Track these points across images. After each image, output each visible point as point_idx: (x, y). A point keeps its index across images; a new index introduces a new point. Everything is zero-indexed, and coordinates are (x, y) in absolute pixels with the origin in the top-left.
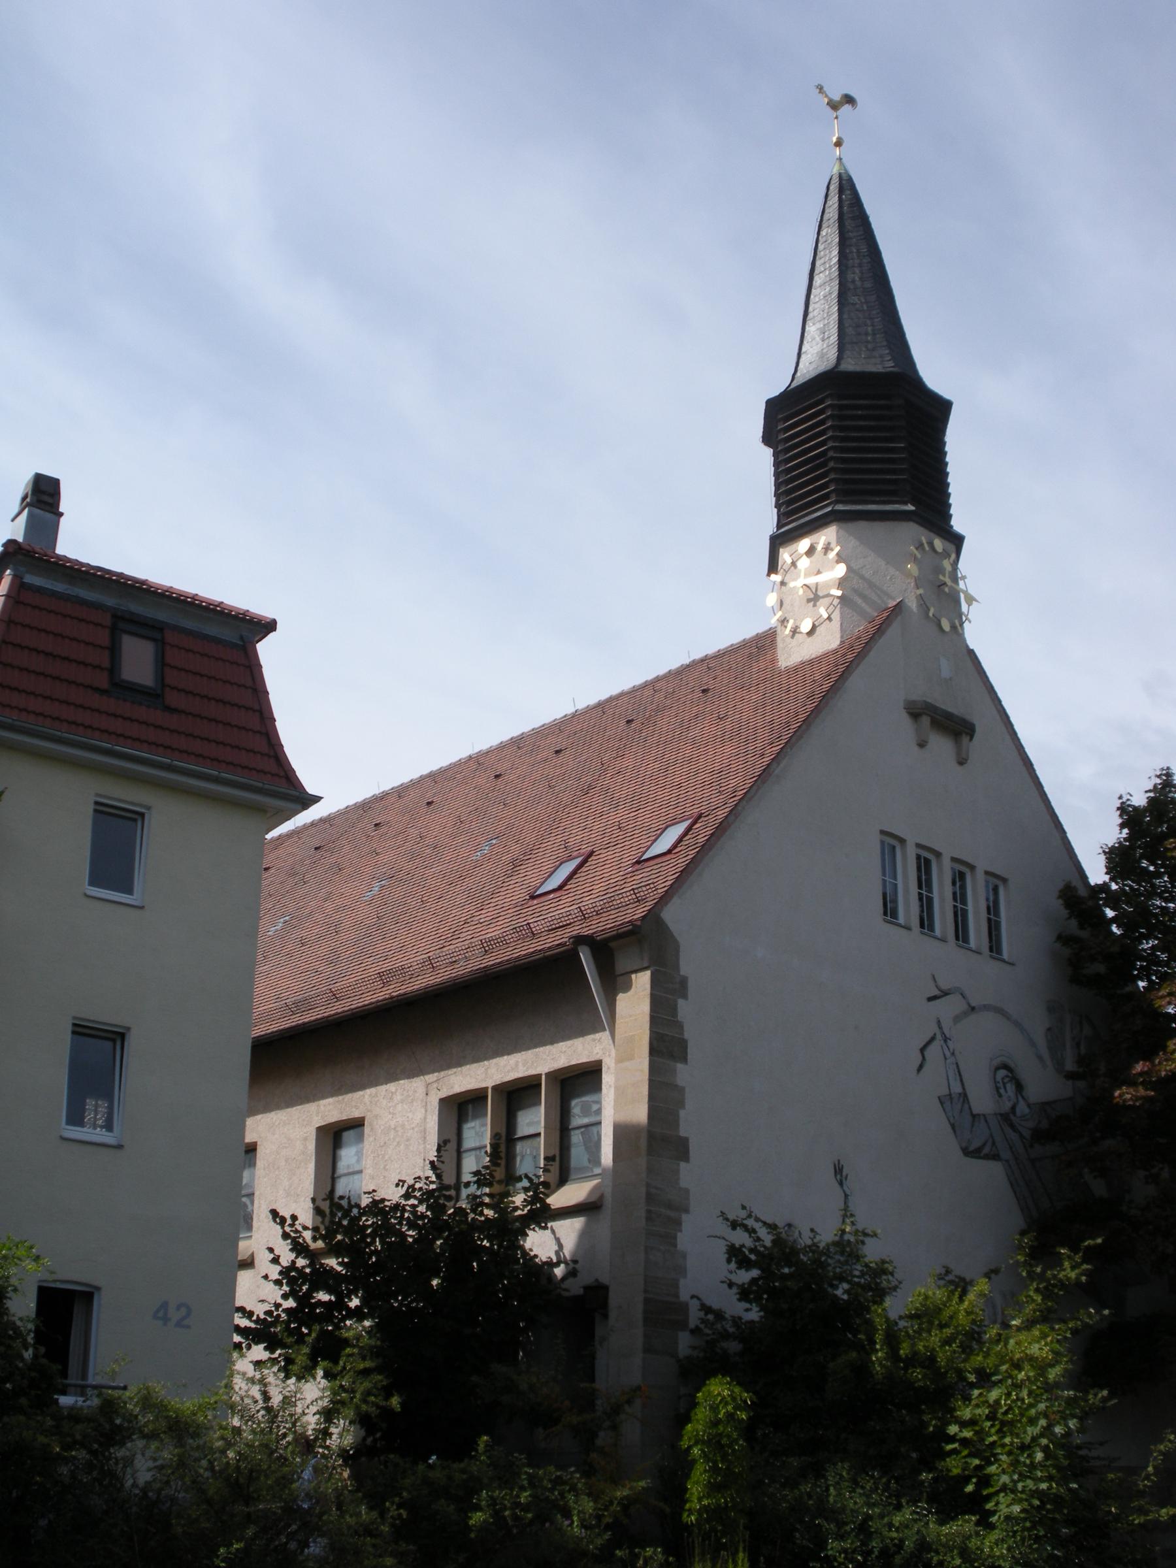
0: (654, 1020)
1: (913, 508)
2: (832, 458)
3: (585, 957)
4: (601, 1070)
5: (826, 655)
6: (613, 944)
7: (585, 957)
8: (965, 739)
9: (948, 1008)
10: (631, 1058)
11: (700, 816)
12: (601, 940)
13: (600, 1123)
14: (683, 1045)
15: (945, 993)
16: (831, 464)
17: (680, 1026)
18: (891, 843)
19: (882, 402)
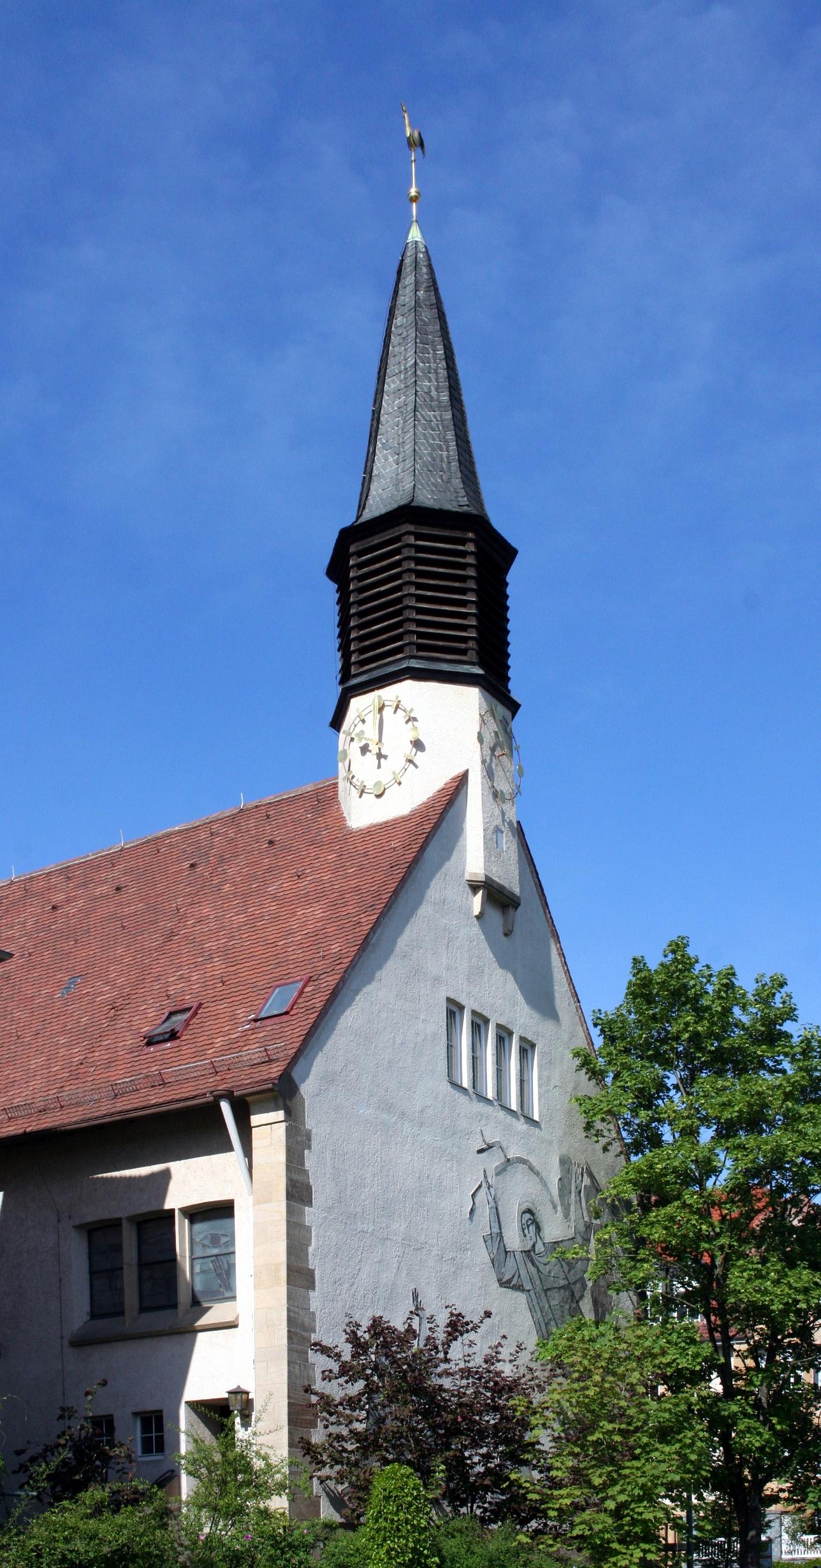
0: (289, 1168)
1: (481, 672)
2: (409, 571)
3: (225, 1107)
4: (233, 1207)
5: (405, 819)
6: (248, 1099)
7: (225, 1107)
8: (511, 911)
9: (493, 1161)
10: (268, 1200)
11: (310, 979)
12: (238, 1097)
13: (234, 1253)
14: (309, 1188)
15: (490, 1147)
16: (406, 552)
17: (306, 1173)
18: (454, 1009)
19: (457, 584)
